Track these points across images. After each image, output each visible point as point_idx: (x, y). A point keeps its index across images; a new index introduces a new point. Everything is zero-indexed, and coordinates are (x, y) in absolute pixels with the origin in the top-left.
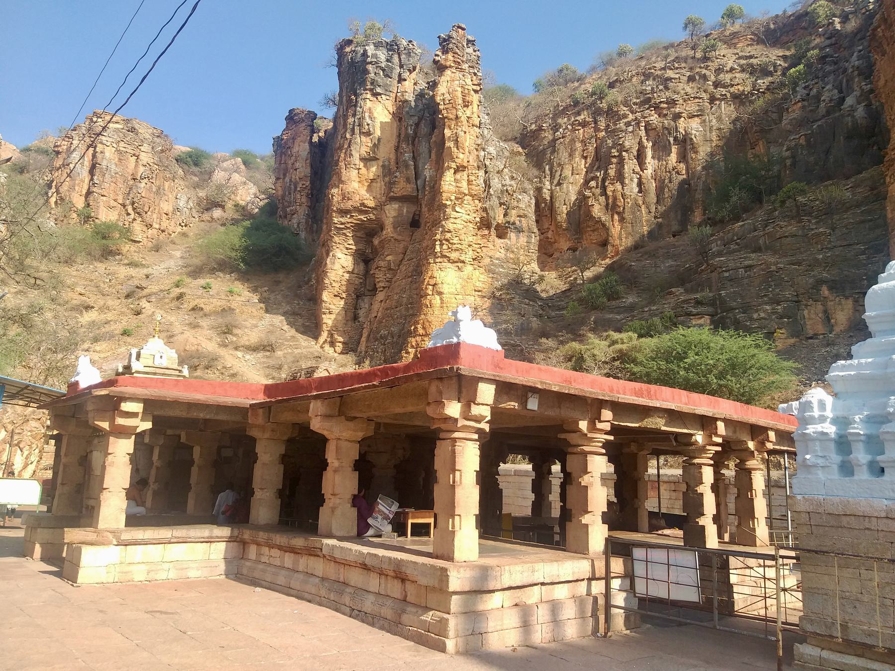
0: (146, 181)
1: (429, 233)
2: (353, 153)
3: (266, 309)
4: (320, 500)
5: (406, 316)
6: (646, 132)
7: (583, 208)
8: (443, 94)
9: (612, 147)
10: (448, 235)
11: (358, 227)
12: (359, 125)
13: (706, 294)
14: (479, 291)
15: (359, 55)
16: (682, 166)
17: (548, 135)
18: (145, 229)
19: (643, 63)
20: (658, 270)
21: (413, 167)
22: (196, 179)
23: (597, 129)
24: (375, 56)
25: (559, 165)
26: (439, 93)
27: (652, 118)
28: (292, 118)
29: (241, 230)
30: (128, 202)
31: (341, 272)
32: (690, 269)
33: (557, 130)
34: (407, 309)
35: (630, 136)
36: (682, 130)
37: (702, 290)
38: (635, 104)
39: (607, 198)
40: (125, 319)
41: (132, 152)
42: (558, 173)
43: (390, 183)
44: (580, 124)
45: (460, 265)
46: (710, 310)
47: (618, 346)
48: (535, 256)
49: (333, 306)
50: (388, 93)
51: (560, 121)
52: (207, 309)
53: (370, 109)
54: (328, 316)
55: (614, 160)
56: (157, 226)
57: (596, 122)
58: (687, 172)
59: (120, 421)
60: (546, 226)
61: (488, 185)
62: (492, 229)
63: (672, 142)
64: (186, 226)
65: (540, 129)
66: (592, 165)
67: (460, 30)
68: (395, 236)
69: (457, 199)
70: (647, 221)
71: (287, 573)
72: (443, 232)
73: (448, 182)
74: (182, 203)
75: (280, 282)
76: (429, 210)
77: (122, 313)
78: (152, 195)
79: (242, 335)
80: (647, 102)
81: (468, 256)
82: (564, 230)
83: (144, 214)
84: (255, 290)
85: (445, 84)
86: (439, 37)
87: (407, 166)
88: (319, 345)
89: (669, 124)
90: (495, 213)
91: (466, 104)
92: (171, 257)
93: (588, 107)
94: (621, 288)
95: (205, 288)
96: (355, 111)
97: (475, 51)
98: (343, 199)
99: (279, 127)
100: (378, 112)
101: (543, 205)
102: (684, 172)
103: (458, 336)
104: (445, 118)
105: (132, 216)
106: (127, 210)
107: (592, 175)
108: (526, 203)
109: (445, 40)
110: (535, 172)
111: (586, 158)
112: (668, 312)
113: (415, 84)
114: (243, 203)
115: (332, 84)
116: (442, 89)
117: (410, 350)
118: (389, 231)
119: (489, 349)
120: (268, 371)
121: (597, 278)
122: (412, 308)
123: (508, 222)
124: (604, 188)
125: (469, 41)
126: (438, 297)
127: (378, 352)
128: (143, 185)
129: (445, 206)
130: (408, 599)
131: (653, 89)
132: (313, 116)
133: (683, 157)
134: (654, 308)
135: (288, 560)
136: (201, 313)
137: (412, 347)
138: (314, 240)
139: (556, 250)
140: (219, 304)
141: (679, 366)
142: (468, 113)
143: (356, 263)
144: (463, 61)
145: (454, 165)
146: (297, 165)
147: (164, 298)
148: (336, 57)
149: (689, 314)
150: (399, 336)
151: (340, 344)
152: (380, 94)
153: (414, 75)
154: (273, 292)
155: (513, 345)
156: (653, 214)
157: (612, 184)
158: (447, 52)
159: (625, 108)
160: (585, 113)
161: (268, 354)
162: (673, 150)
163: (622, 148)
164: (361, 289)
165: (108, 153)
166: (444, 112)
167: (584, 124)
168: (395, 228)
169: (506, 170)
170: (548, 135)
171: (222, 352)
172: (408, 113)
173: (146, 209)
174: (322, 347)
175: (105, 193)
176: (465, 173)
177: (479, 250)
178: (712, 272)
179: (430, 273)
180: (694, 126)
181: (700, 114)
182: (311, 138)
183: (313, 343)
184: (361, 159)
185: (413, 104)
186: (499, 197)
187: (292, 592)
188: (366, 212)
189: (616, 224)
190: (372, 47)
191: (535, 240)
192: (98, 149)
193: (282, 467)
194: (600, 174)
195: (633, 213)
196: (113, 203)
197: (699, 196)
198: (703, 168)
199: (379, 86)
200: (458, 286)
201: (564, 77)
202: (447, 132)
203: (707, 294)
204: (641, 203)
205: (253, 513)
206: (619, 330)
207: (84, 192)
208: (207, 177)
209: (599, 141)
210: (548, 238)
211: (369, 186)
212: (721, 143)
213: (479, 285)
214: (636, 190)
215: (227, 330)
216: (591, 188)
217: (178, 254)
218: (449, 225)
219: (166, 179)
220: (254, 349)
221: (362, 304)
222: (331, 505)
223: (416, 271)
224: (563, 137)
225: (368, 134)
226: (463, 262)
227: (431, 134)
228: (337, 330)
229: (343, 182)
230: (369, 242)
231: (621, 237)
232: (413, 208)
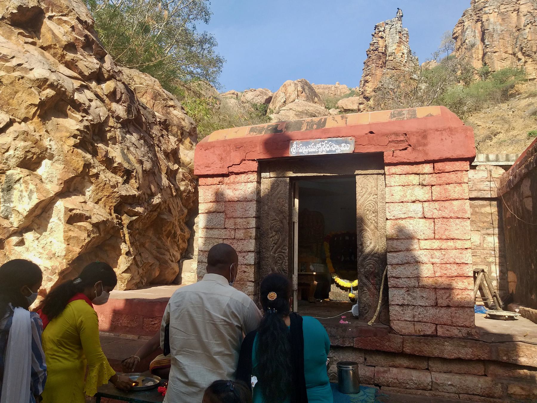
0: (529, 26)
30: (517, 50)
41: (512, 9)
83: (533, 54)
105: (523, 60)
106: (517, 57)
128: (527, 30)
165: (492, 19)
175: (496, 50)
192: (484, 20)
196: (504, 55)
207: (480, 56)
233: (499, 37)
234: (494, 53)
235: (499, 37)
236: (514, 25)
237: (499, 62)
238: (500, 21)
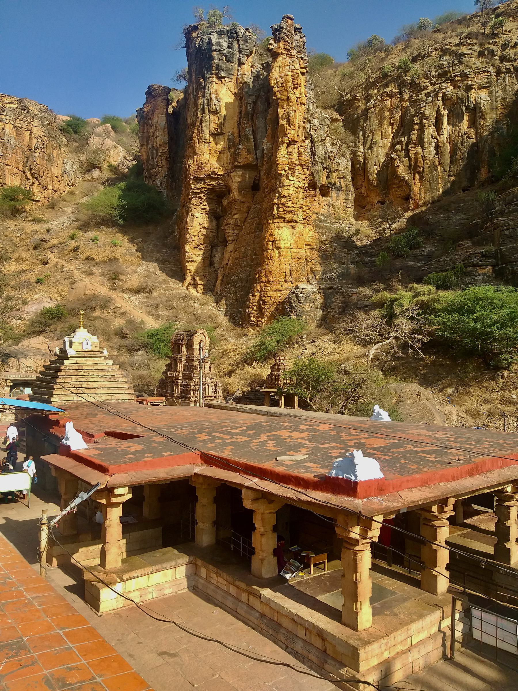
0: (39, 151)
1: (268, 197)
2: (204, 129)
3: (142, 257)
4: (252, 552)
5: (251, 265)
6: (443, 102)
7: (390, 168)
8: (277, 79)
9: (415, 115)
10: (284, 200)
11: (211, 191)
12: (208, 105)
13: (490, 248)
14: (309, 245)
15: (205, 43)
16: (472, 131)
17: (361, 105)
18: (42, 190)
19: (441, 36)
20: (451, 221)
21: (252, 140)
22: (77, 144)
23: (402, 100)
24: (218, 44)
25: (371, 131)
26: (273, 77)
27: (448, 90)
28: (150, 93)
29: (118, 193)
30: (27, 169)
31: (198, 228)
32: (476, 224)
33: (369, 101)
34: (252, 260)
35: (429, 106)
36: (472, 100)
37: (486, 244)
38: (433, 76)
39: (410, 159)
40: (37, 268)
42: (370, 138)
43: (234, 153)
44: (388, 95)
45: (293, 224)
46: (492, 261)
47: (421, 298)
48: (351, 210)
49: (194, 257)
50: (230, 76)
51: (371, 92)
52: (97, 258)
53: (216, 91)
54: (190, 263)
55: (416, 127)
56: (51, 188)
57: (401, 93)
58: (476, 137)
59: (114, 500)
60: (360, 183)
61: (313, 153)
62: (318, 190)
63: (464, 110)
64: (73, 185)
65: (355, 98)
66: (398, 131)
67: (289, 20)
68: (240, 198)
69: (290, 169)
70: (442, 179)
71: (233, 600)
72: (280, 197)
73: (283, 155)
74: (68, 167)
75: (150, 233)
76: (267, 178)
77: (34, 263)
78: (45, 162)
79: (126, 280)
80: (443, 75)
81: (299, 217)
82: (375, 186)
83: (40, 178)
84: (132, 241)
85: (278, 69)
87: (248, 139)
88: (184, 287)
89: (462, 95)
90: (320, 177)
91: (296, 87)
92: (64, 213)
93: (394, 80)
94: (420, 239)
95: (93, 241)
96: (204, 93)
97: (301, 38)
98: (198, 168)
99: (140, 101)
100: (223, 93)
101: (358, 166)
102: (474, 136)
103: (356, 476)
104: (278, 99)
105: (31, 180)
106: (26, 176)
107: (398, 140)
108: (344, 165)
109: (277, 30)
110: (351, 138)
111: (392, 125)
112: (460, 264)
113: (252, 66)
114: (115, 164)
115: (182, 64)
116: (275, 74)
117: (256, 294)
118: (235, 194)
119: (376, 480)
120: (149, 309)
121: (401, 230)
122: (256, 259)
123: (330, 183)
124: (407, 151)
125: (296, 29)
126: (276, 251)
127: (230, 294)
128: (37, 154)
129: (281, 175)
130: (327, 652)
131: (449, 63)
132: (167, 91)
133: (473, 124)
134: (448, 258)
135: (233, 590)
136: (93, 262)
137: (258, 291)
138: (173, 196)
139: (368, 203)
140: (106, 254)
141: (469, 318)
142: (297, 94)
143: (210, 219)
144: (292, 48)
145: (286, 140)
146: (157, 133)
147: (63, 249)
148: (185, 39)
149: (476, 265)
150: (247, 281)
151: (201, 287)
152: (224, 77)
153: (251, 59)
154: (146, 242)
155: (336, 289)
156: (447, 173)
157: (414, 148)
158: (279, 41)
159: (426, 81)
160: (393, 85)
161: (147, 295)
162: (465, 117)
163: (423, 116)
164: (215, 241)
166: (278, 94)
167: (391, 95)
168: (240, 191)
169: (328, 138)
170: (361, 105)
171: (113, 295)
172: (247, 92)
173: (41, 174)
174: (187, 289)
175: (9, 163)
176: (296, 147)
177: (308, 211)
178: (495, 229)
179: (269, 231)
180: (483, 97)
181: (488, 85)
182: (167, 110)
183: (180, 285)
184: (211, 135)
185: (251, 85)
186: (322, 163)
187: (237, 615)
188: (216, 179)
189: (417, 181)
190: (216, 35)
191: (351, 197)
193: (215, 505)
194: (404, 139)
195: (431, 172)
196: (15, 171)
197: (485, 157)
198: (490, 133)
199: (223, 70)
200: (292, 241)
201: (372, 46)
202: (281, 111)
203: (490, 248)
204: (437, 163)
205: (198, 537)
206: (419, 281)
208: (85, 142)
209: (403, 110)
210: (361, 193)
211: (218, 158)
212: (505, 112)
213: (309, 240)
214: (434, 152)
215: (114, 277)
216: (396, 151)
217: (69, 210)
218: (284, 191)
219: (54, 148)
220: (136, 291)
221: (216, 253)
222: (260, 557)
223: (258, 228)
224: (374, 107)
225: (216, 113)
226: (296, 222)
227: (266, 111)
228: (198, 275)
229: (197, 154)
230: (220, 203)
231: (421, 193)
232: (254, 174)
233: (12, 151)
234: (7, 165)
235: (12, 151)
236: (27, 145)
237: (10, 176)
238: (15, 134)
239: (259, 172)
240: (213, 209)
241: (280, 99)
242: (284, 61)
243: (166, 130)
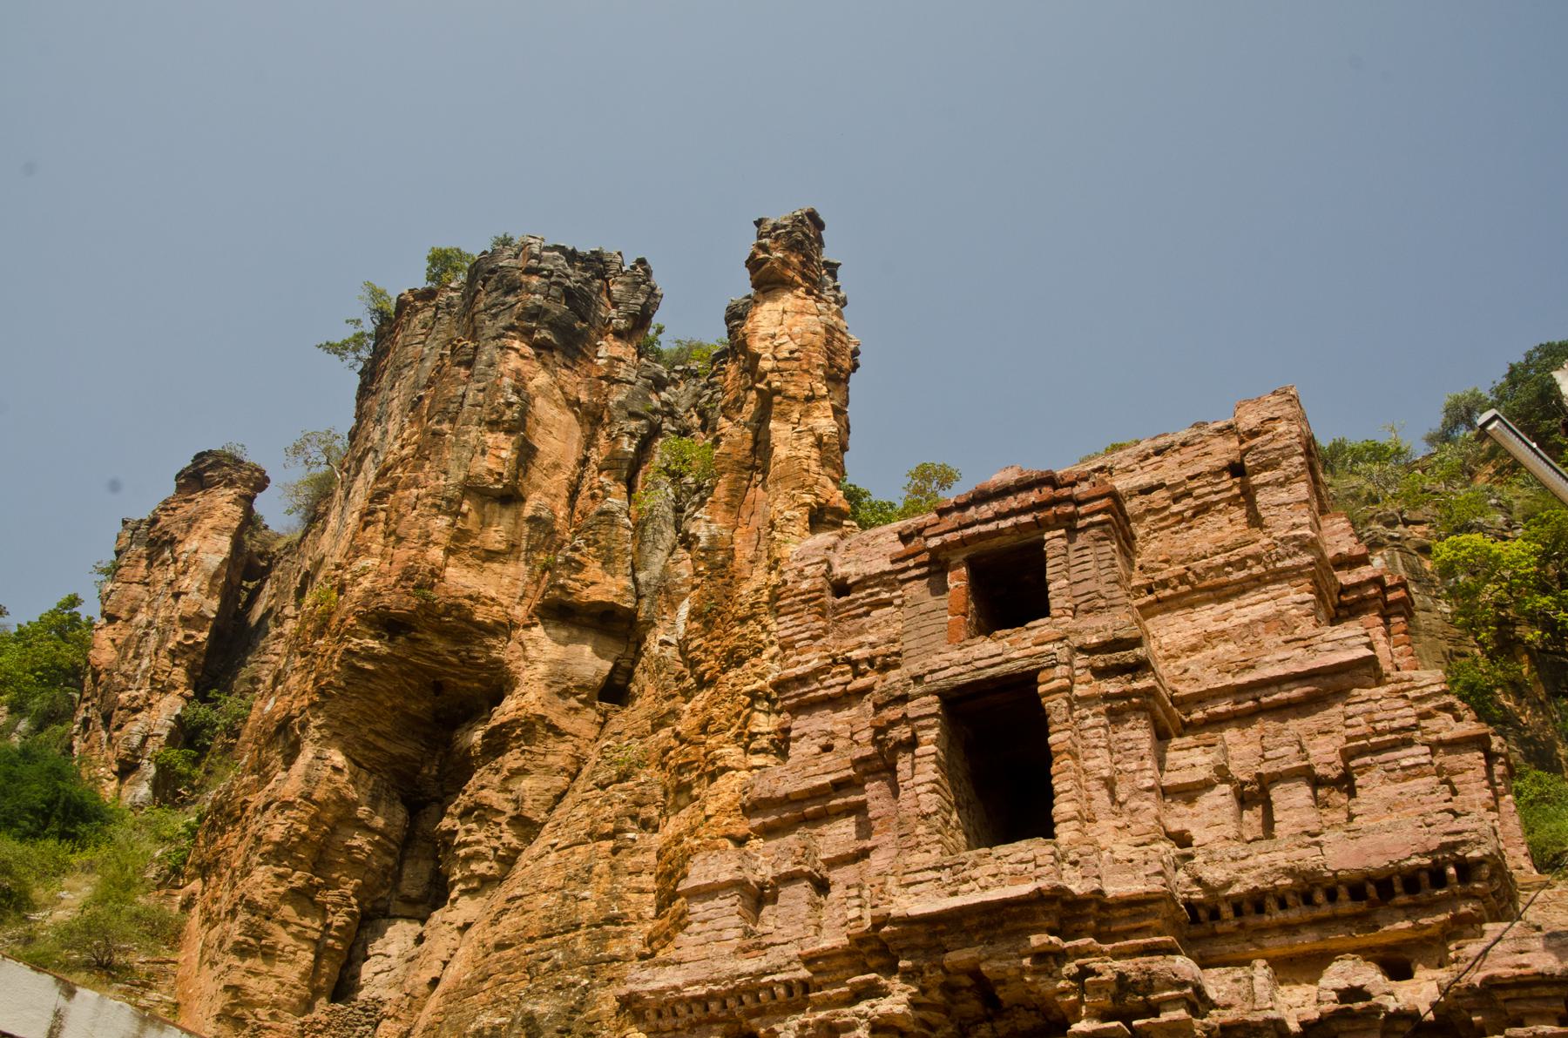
28: (199, 476)
86: (759, 223)
223: (634, 818)
239: (633, 647)
240: (403, 758)
241: (778, 392)
242: (800, 302)
243: (220, 582)
